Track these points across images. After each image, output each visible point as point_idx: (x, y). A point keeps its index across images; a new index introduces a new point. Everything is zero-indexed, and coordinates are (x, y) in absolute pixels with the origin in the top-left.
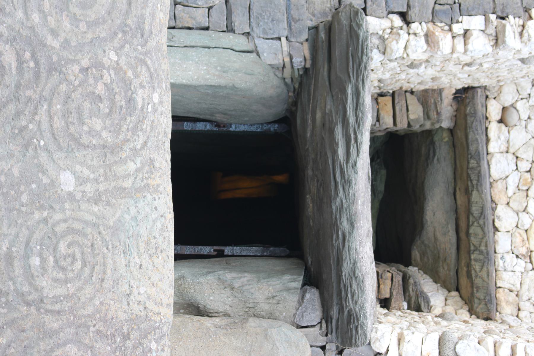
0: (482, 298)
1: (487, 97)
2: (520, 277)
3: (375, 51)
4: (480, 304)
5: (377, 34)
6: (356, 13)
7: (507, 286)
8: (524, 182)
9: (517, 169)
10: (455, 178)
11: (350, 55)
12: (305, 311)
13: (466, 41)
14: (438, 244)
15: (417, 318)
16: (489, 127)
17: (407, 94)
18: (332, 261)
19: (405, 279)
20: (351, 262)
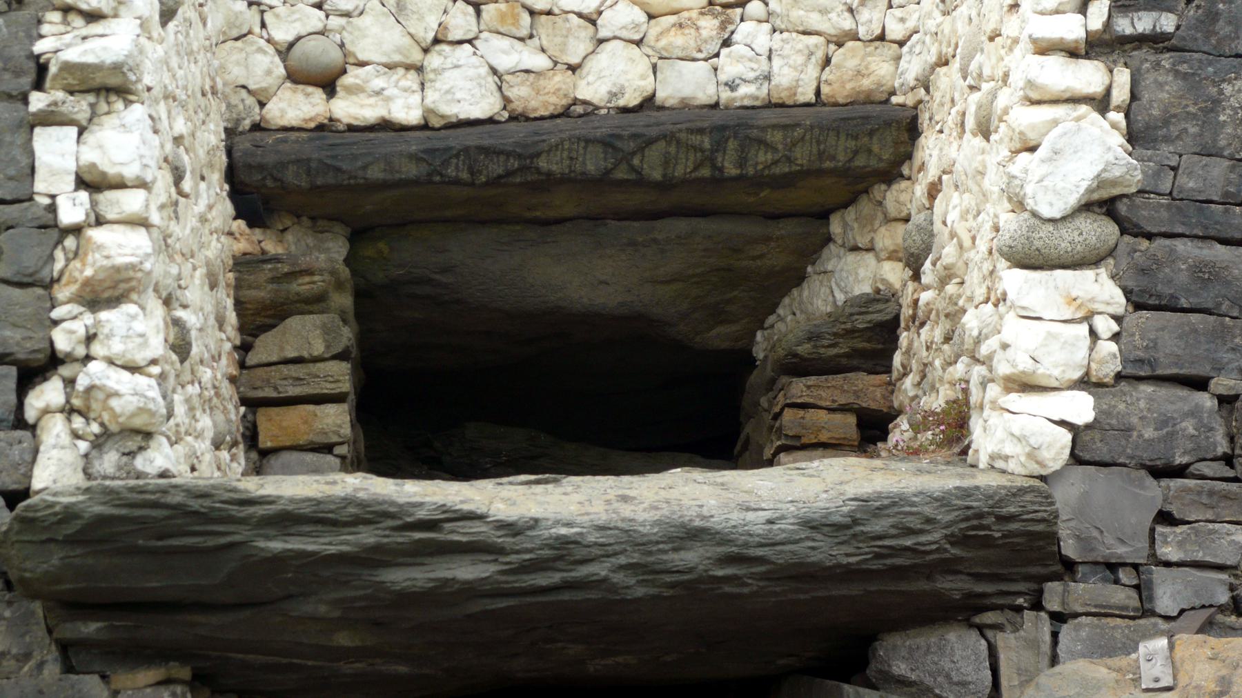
0: (852, 144)
1: (256, 127)
2: (785, 35)
3: (140, 463)
4: (870, 151)
5: (86, 456)
6: (26, 522)
7: (812, 72)
8: (510, 21)
9: (470, 42)
10: (499, 222)
11: (160, 543)
12: (948, 676)
13: (113, 182)
14: (690, 272)
15: (932, 333)
16: (346, 120)
17: (252, 359)
18: (802, 597)
20: (807, 538)
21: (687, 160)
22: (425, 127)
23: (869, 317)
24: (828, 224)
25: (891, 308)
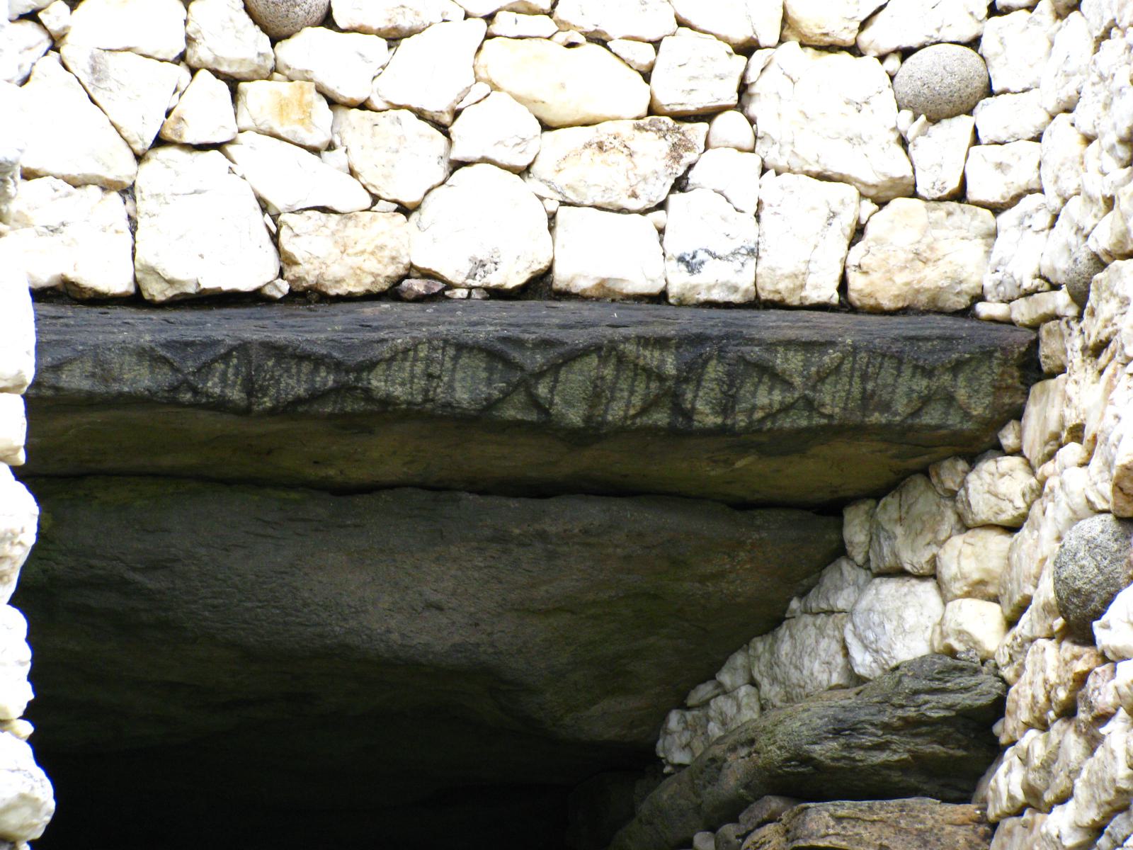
0: (921, 384)
4: (950, 399)
8: (296, 114)
9: (218, 146)
10: (255, 483)
14: (590, 596)
19: (805, 782)
21: (632, 392)
22: (136, 299)
23: (949, 699)
24: (840, 527)
25: (987, 687)
